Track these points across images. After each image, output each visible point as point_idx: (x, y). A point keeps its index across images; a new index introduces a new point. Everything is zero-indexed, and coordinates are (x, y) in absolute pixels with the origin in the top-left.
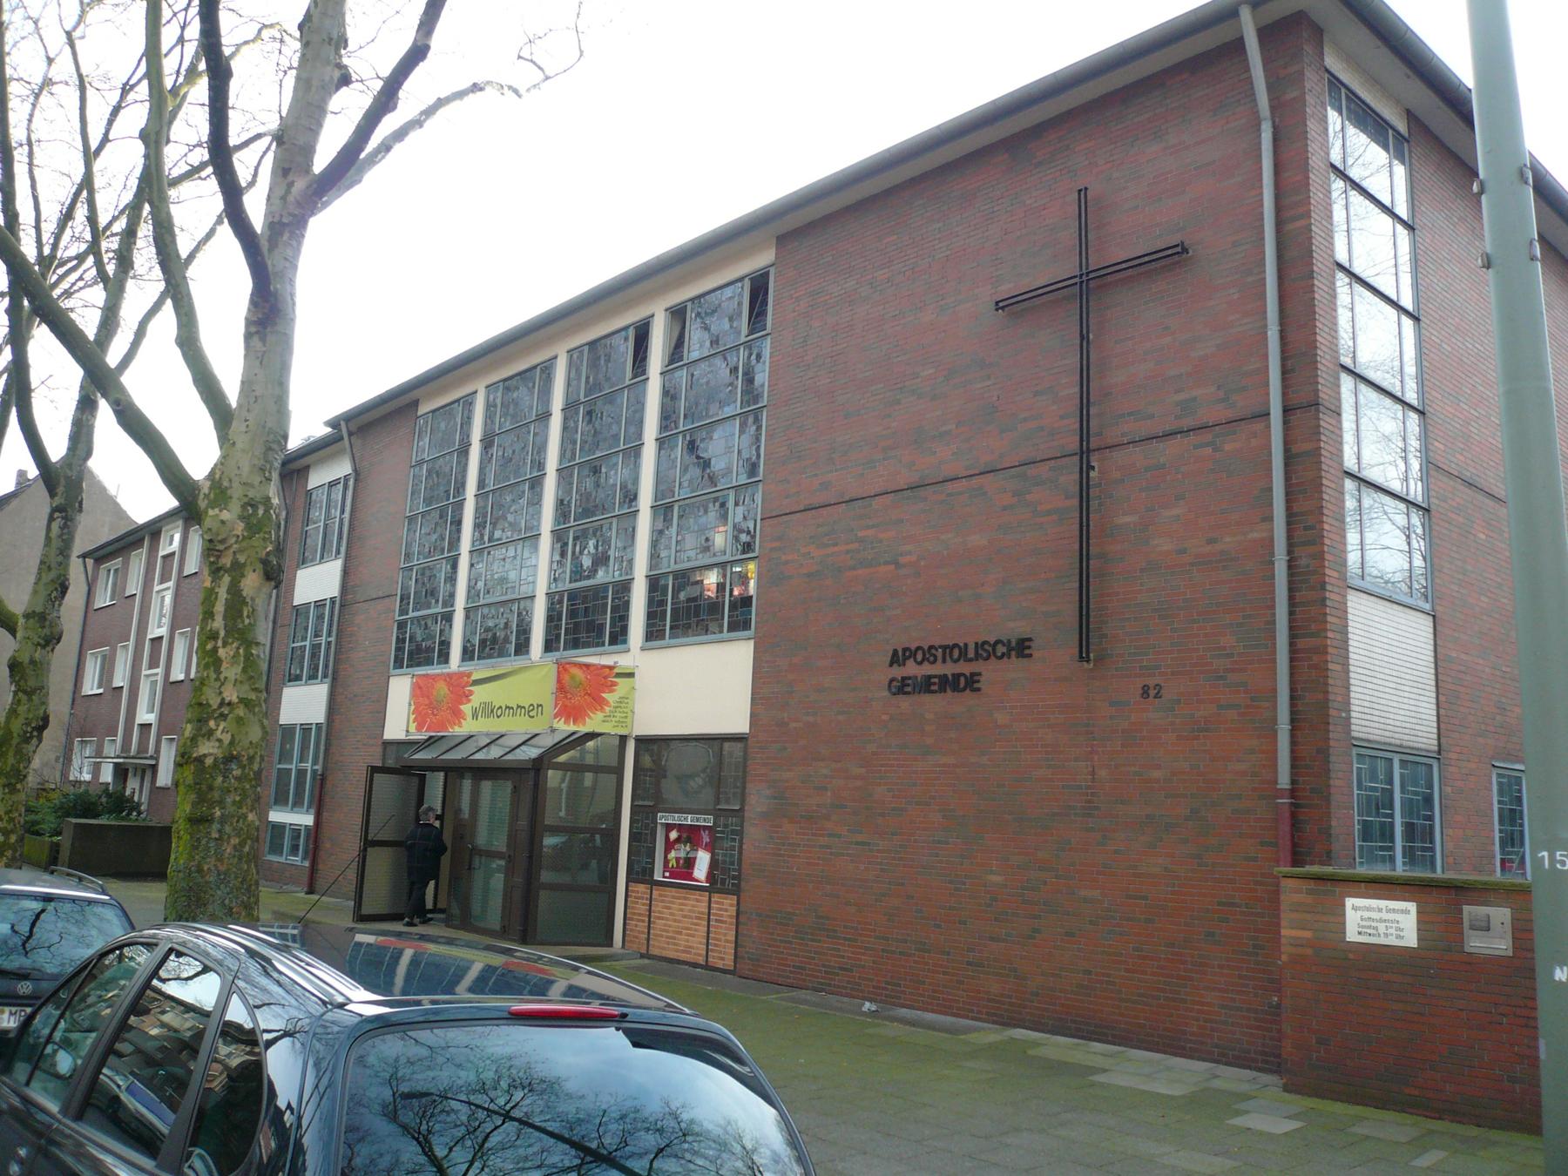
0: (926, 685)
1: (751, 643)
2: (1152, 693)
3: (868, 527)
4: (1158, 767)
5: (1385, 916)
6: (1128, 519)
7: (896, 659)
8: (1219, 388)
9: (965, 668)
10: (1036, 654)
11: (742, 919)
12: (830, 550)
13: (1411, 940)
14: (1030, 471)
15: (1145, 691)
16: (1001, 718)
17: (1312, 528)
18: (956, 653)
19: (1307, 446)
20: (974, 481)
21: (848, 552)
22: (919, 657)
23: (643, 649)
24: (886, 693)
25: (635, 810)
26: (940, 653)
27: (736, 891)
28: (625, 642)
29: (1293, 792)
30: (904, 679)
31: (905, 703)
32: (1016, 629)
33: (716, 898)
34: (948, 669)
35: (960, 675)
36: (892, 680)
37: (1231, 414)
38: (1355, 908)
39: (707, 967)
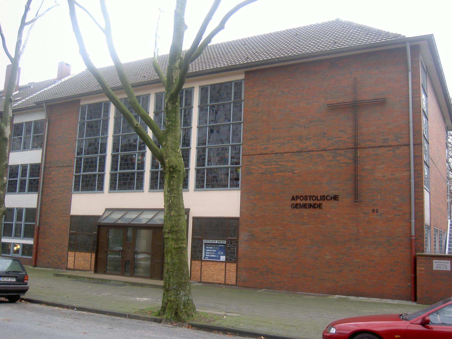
0: (304, 206)
1: (240, 191)
2: (375, 211)
3: (283, 162)
4: (377, 229)
5: (443, 264)
6: (368, 167)
7: (293, 199)
8: (395, 137)
9: (318, 202)
10: (340, 200)
11: (238, 270)
12: (269, 167)
13: (449, 269)
14: (338, 151)
15: (373, 211)
16: (329, 216)
17: (420, 174)
18: (314, 198)
19: (419, 154)
20: (320, 152)
21: (275, 168)
22: (302, 198)
23: (194, 191)
24: (290, 208)
25: (193, 239)
26: (308, 198)
27: (236, 262)
28: (187, 188)
29: (415, 236)
30: (296, 204)
31: (297, 211)
32: (333, 193)
33: (228, 264)
34: (312, 202)
35: (315, 204)
36: (292, 204)
37: (398, 144)
38: (435, 262)
39: (225, 284)
